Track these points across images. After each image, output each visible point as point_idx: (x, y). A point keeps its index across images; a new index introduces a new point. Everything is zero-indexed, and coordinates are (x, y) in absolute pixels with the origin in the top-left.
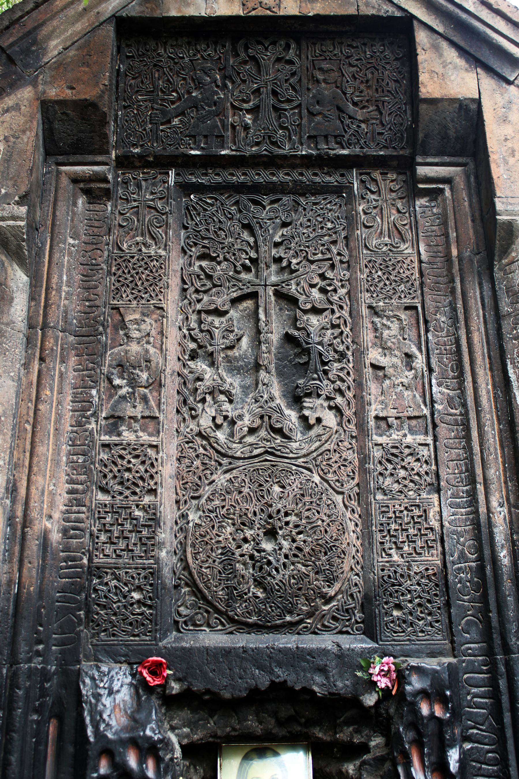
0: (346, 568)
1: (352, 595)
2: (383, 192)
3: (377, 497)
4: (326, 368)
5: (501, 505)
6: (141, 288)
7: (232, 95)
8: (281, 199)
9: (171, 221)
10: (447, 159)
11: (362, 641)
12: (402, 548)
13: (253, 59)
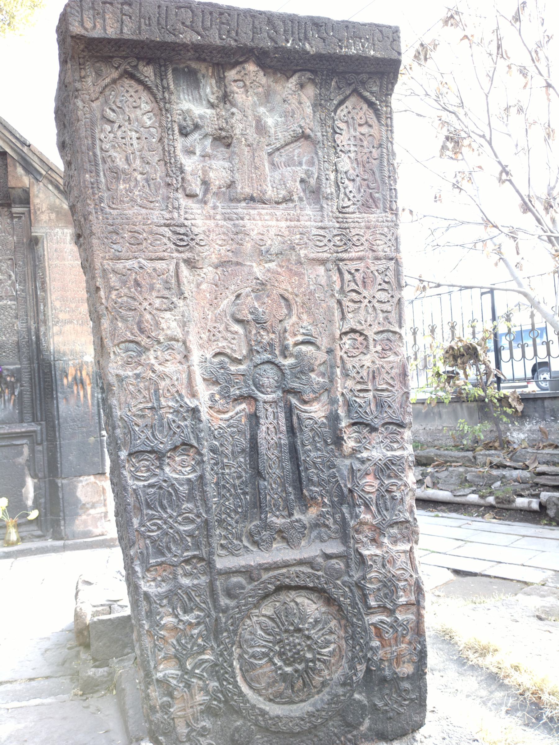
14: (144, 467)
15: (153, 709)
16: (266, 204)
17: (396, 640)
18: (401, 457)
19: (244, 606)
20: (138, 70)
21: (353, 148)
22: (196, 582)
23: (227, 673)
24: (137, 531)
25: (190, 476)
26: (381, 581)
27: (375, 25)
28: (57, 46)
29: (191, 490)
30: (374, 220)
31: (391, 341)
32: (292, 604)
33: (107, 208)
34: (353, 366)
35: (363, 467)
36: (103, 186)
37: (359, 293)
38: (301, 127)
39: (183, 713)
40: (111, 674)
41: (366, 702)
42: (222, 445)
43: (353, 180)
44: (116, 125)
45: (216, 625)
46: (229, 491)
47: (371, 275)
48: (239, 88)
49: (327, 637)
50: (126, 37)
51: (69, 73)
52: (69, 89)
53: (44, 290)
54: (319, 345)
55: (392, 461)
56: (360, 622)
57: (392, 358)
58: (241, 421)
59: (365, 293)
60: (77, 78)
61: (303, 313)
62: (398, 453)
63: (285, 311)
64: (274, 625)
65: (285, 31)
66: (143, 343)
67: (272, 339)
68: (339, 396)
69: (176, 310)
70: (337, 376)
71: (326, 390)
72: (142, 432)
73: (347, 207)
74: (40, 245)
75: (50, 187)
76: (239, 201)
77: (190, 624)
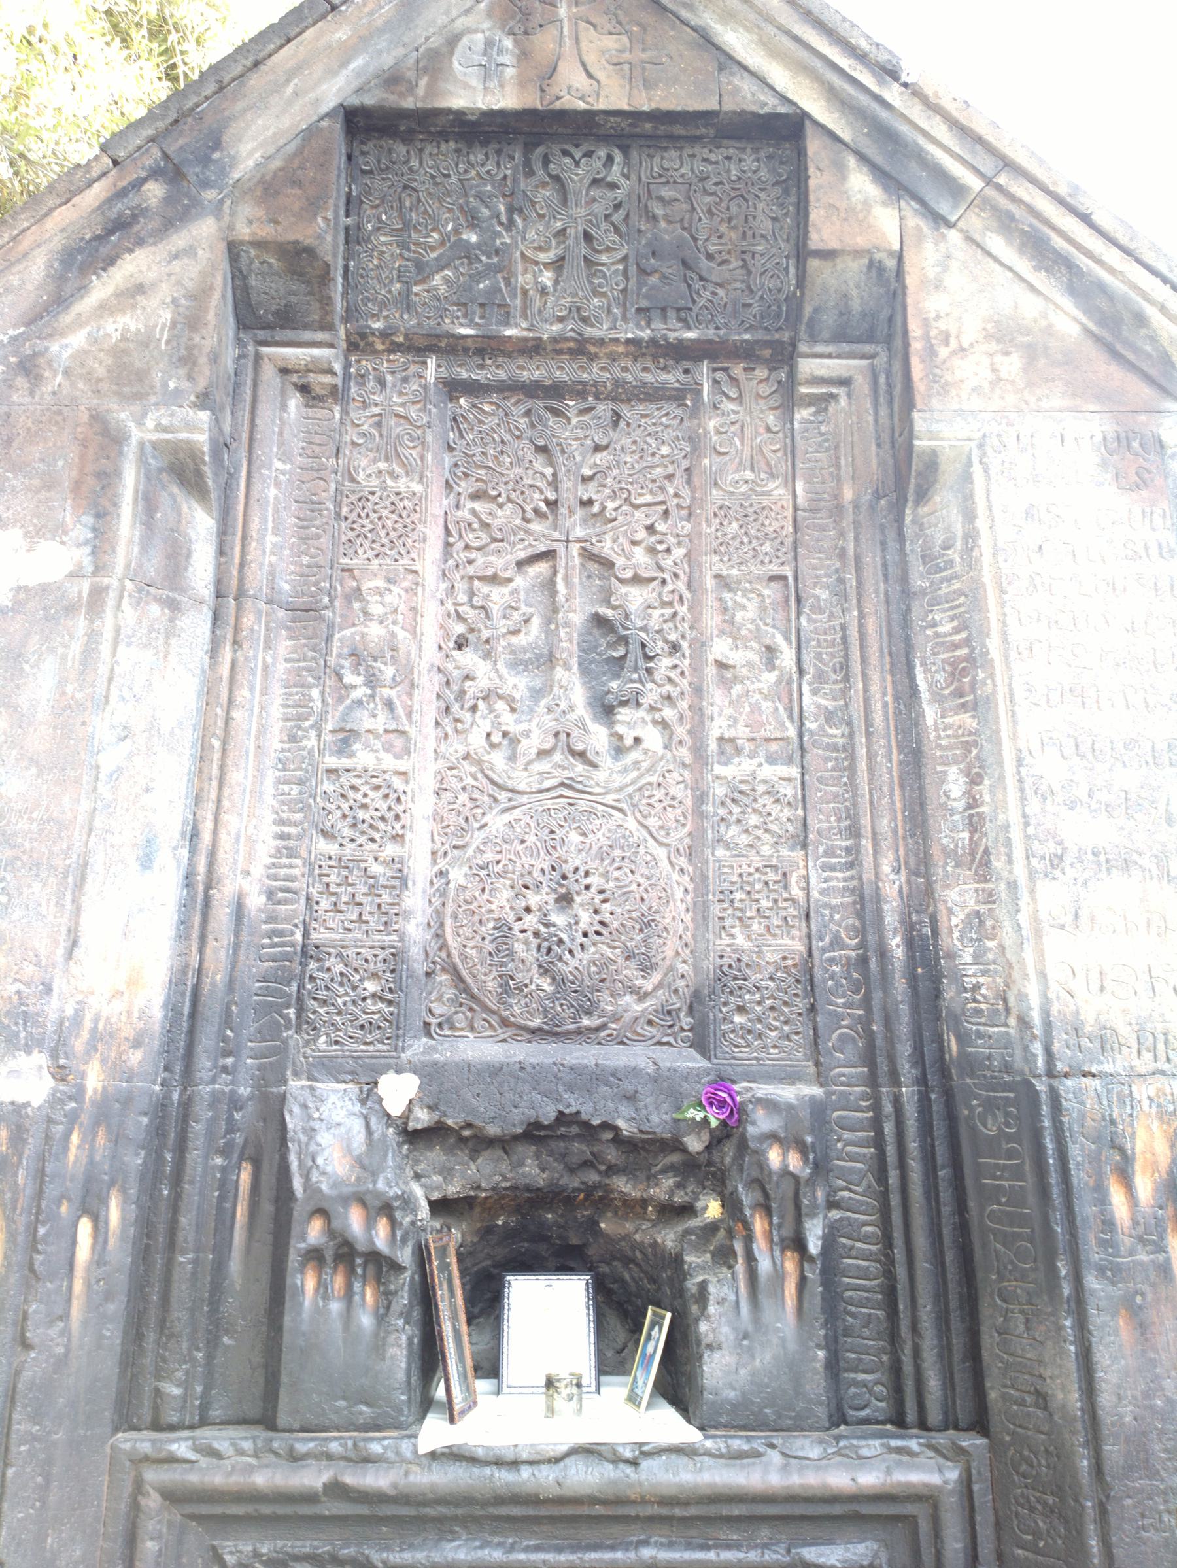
0: (669, 952)
1: (676, 991)
2: (746, 399)
3: (717, 853)
4: (651, 665)
5: (897, 871)
6: (385, 541)
7: (524, 239)
8: (593, 409)
9: (429, 438)
10: (846, 347)
11: (691, 1059)
12: (748, 926)
13: (557, 179)
75: (996, 243)
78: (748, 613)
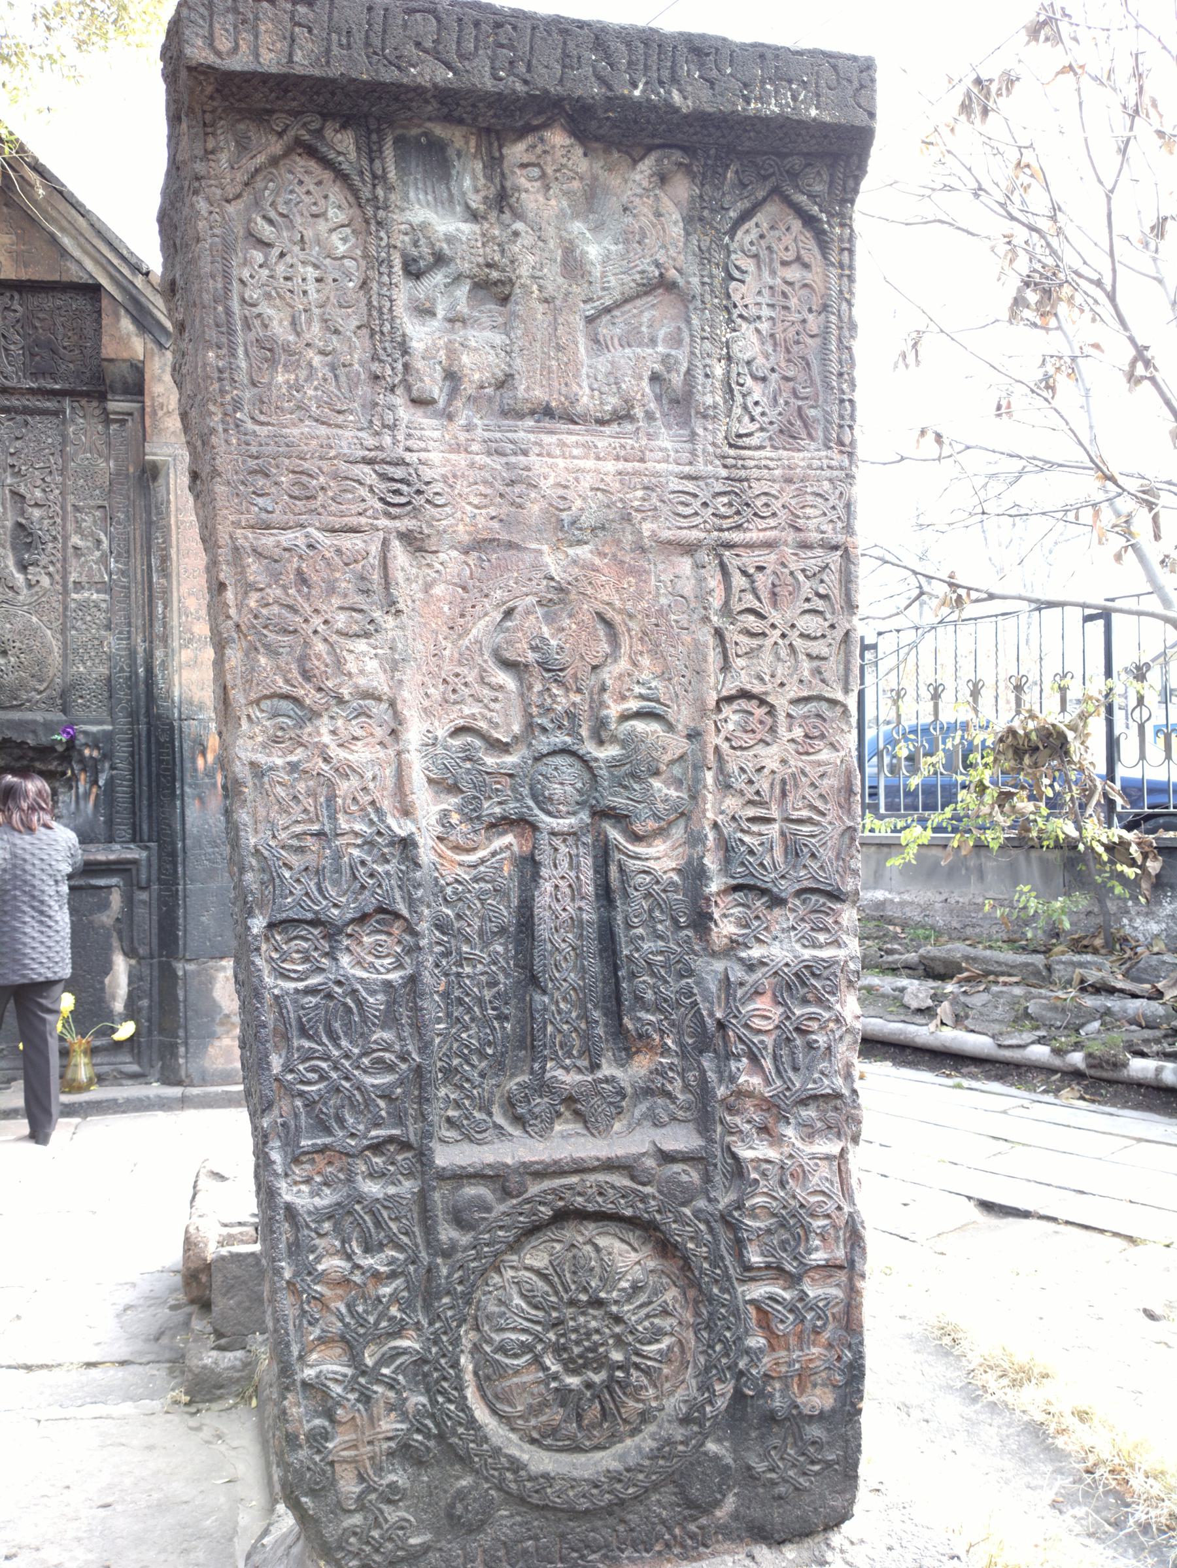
14: (298, 952)
15: (291, 1440)
16: (576, 423)
17: (800, 1338)
18: (831, 963)
19: (487, 1245)
20: (324, 137)
21: (766, 312)
22: (391, 1190)
23: (445, 1379)
24: (276, 1080)
25: (390, 977)
26: (774, 1215)
27: (823, 53)
28: (162, 87)
29: (391, 1004)
30: (802, 464)
31: (824, 720)
32: (588, 1248)
33: (249, 421)
34: (742, 770)
35: (751, 979)
36: (242, 377)
37: (763, 617)
38: (658, 265)
39: (353, 1453)
40: (249, 1365)
41: (729, 1460)
42: (459, 917)
43: (764, 379)
44: (276, 252)
45: (429, 1280)
46: (469, 1010)
47: (790, 580)
48: (530, 180)
49: (656, 1321)
50: (298, 70)
51: (185, 140)
52: (183, 174)
53: (165, 573)
54: (672, 720)
55: (811, 969)
56: (727, 1296)
57: (825, 755)
58: (502, 870)
59: (775, 616)
60: (199, 152)
61: (641, 653)
62: (826, 953)
63: (606, 647)
64: (547, 1288)
65: (630, 63)
66: (308, 701)
67: (574, 704)
68: (707, 829)
69: (378, 636)
70: (705, 787)
71: (682, 814)
72: (298, 881)
73: (747, 435)
74: (161, 480)
76: (520, 416)
77: (376, 1275)
78: (87, 522)
